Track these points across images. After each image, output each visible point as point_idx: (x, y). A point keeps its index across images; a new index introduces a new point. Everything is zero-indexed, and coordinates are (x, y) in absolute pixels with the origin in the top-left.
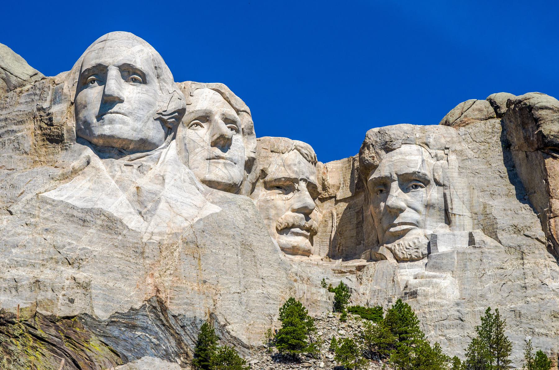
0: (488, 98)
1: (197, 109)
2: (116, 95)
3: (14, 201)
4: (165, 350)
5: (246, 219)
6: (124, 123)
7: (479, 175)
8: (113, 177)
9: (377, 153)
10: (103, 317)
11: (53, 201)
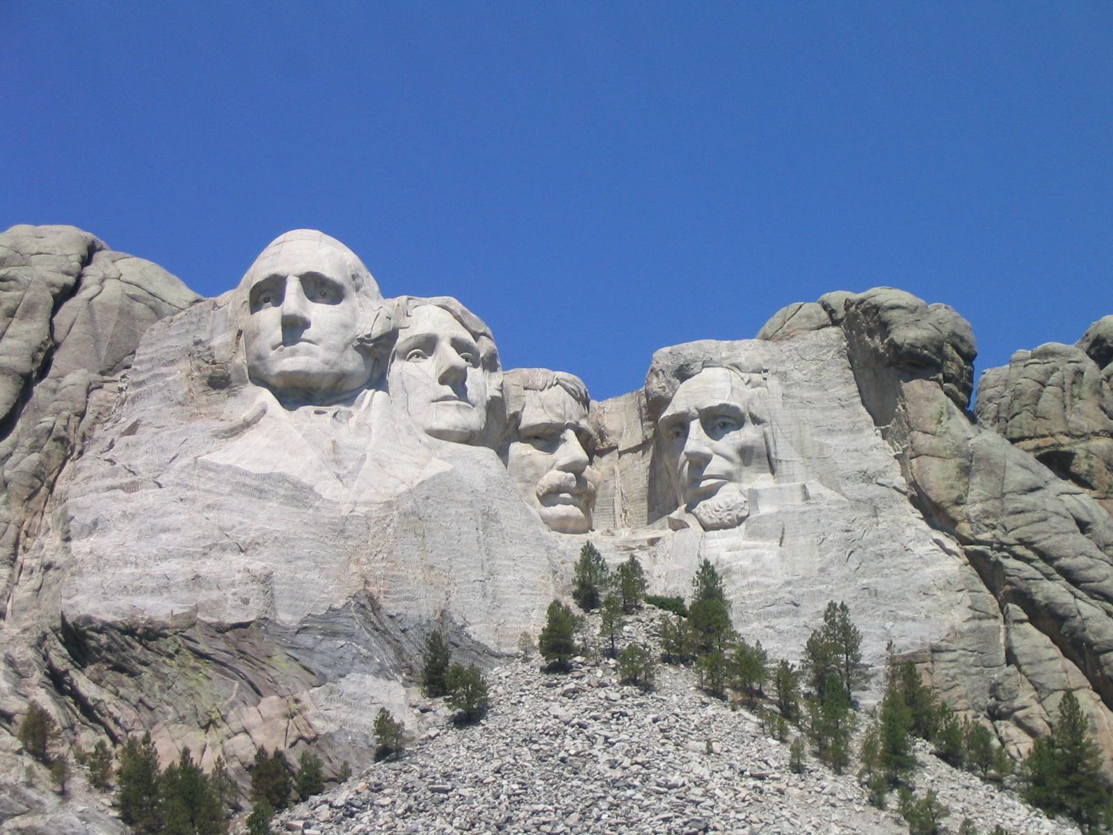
0: (820, 299)
1: (416, 333)
2: (298, 314)
3: (163, 468)
4: (379, 664)
5: (488, 479)
6: (309, 353)
7: (812, 405)
8: (299, 428)
9: (669, 382)
10: (291, 622)
11: (218, 466)
